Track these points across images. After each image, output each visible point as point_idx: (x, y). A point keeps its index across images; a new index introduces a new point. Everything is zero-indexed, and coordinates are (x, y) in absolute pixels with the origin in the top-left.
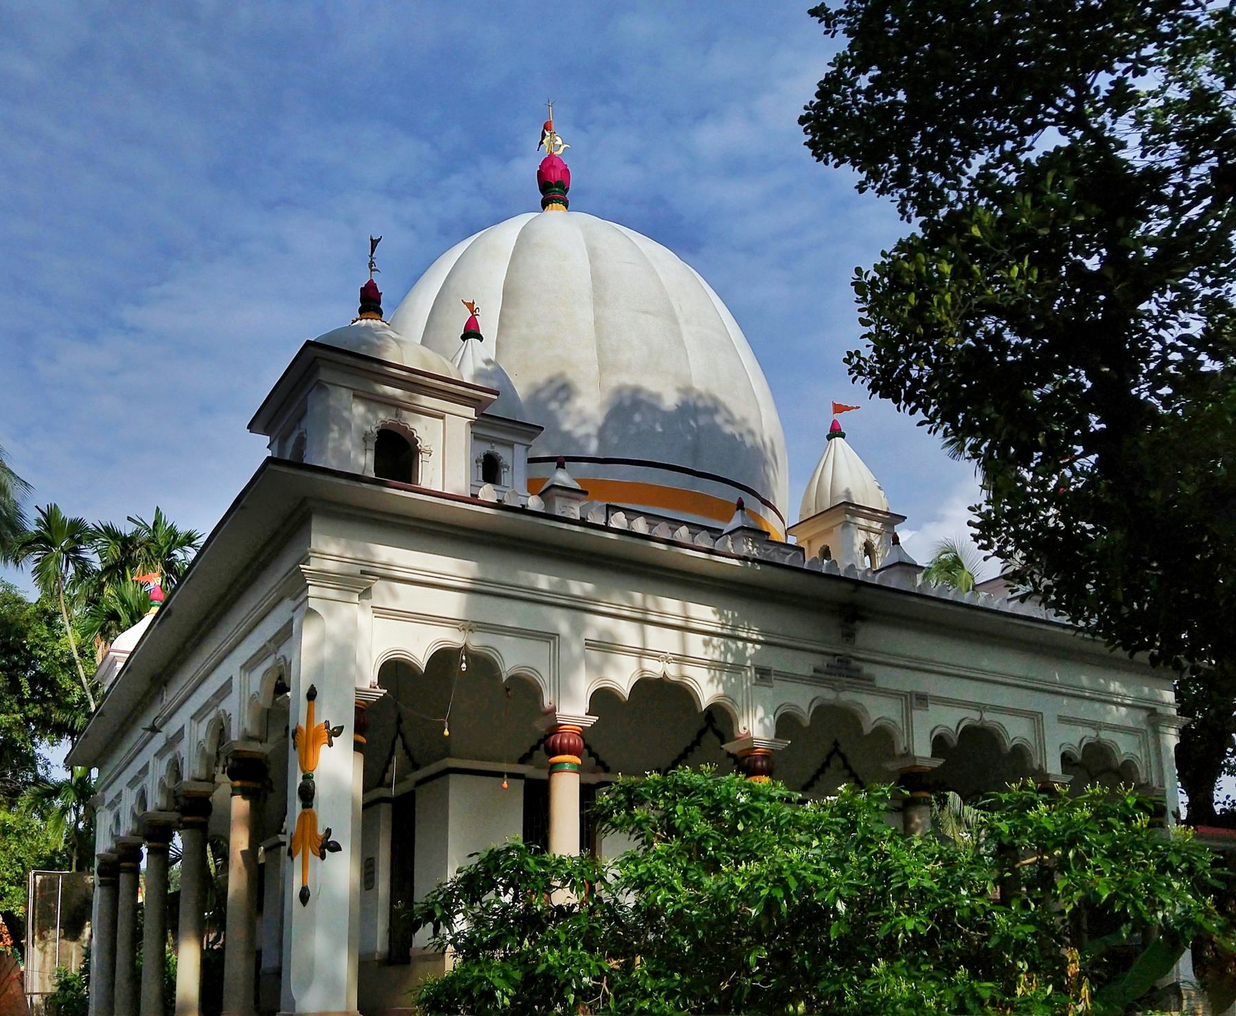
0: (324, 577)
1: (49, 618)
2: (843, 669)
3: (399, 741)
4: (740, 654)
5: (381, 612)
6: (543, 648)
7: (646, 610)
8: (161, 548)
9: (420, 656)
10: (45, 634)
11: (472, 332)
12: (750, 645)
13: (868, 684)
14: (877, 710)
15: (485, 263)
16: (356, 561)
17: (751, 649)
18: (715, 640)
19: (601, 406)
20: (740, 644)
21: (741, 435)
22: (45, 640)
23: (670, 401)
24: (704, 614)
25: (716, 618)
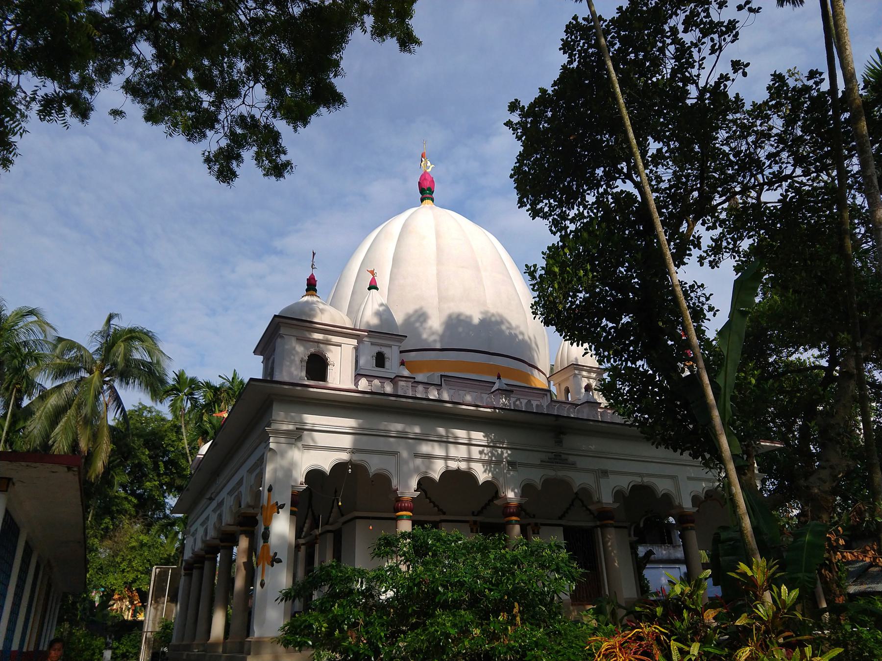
1: (177, 429)
2: (558, 460)
3: (310, 513)
6: (393, 459)
8: (235, 392)
9: (327, 467)
10: (174, 439)
11: (373, 286)
12: (505, 451)
13: (573, 466)
14: (579, 480)
15: (384, 242)
22: (173, 441)
24: (478, 436)
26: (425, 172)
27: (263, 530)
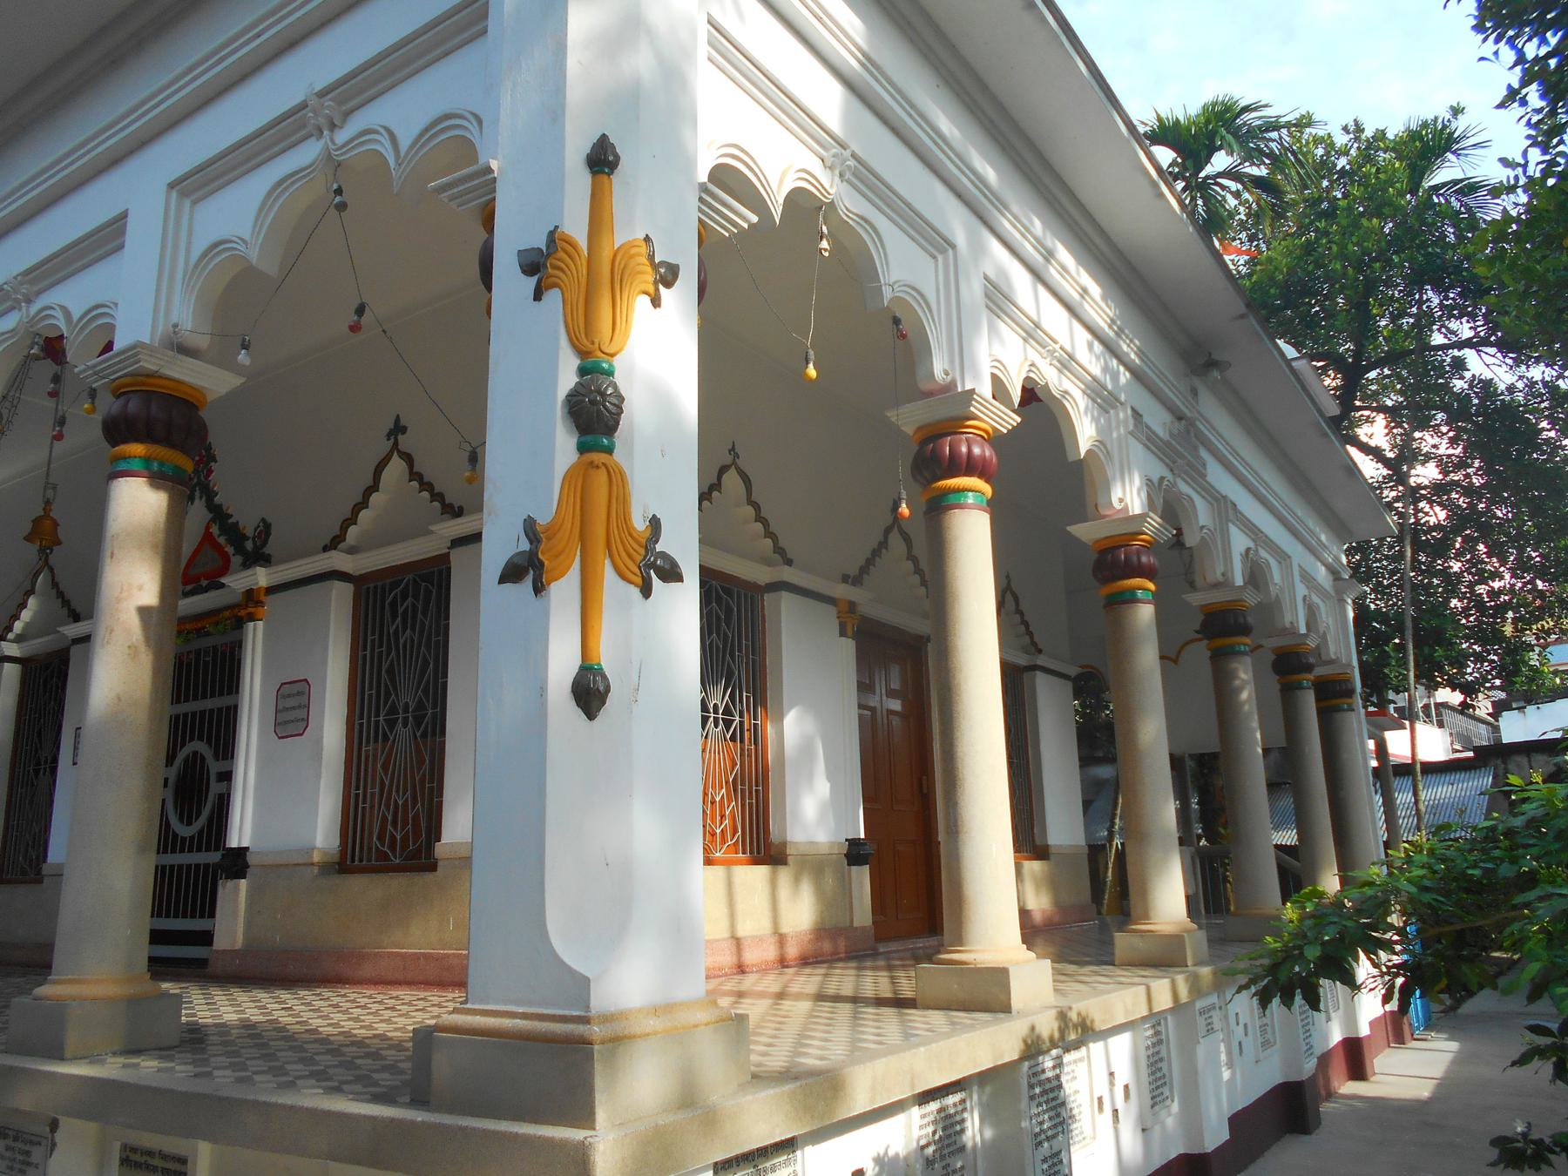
4: (1115, 376)
12: (1122, 369)
17: (1124, 376)
18: (1096, 344)
20: (1115, 362)
27: (568, 379)
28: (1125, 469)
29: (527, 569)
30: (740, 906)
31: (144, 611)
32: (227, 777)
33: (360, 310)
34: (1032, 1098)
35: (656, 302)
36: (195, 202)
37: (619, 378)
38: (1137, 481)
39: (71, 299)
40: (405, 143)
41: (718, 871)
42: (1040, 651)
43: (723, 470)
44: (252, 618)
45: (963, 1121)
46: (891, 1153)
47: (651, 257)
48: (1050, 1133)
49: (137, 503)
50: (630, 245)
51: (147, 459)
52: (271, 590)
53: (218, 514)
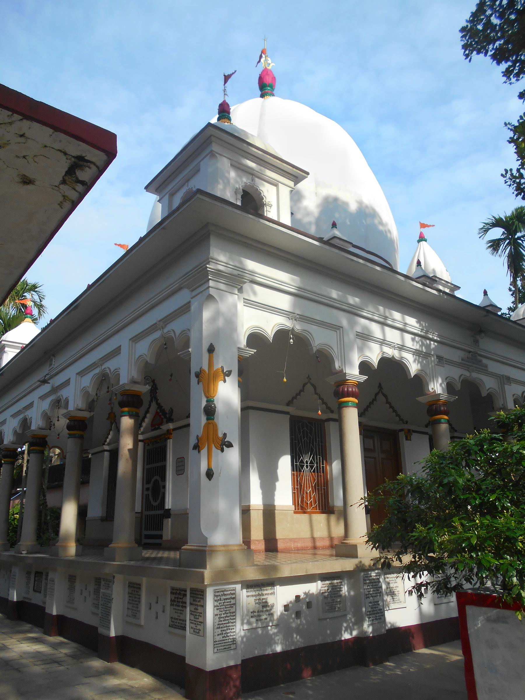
0: (218, 274)
2: (473, 360)
4: (428, 347)
5: (248, 303)
7: (386, 318)
12: (432, 343)
13: (484, 370)
14: (489, 384)
16: (236, 268)
17: (433, 345)
18: (417, 338)
19: (318, 206)
20: (428, 342)
21: (386, 232)
23: (353, 207)
24: (412, 322)
25: (417, 325)
26: (266, 68)
27: (204, 403)
28: (434, 377)
29: (197, 447)
30: (315, 528)
31: (129, 450)
32: (164, 487)
33: (171, 375)
34: (365, 583)
35: (225, 381)
36: (136, 343)
37: (215, 402)
38: (440, 381)
39: (111, 365)
40: (177, 335)
41: (304, 517)
42: (456, 431)
43: (304, 385)
44: (169, 438)
45: (341, 588)
46: (310, 592)
47: (223, 370)
48: (373, 595)
49: (127, 422)
50: (218, 369)
51: (129, 412)
52: (174, 430)
53: (159, 406)
